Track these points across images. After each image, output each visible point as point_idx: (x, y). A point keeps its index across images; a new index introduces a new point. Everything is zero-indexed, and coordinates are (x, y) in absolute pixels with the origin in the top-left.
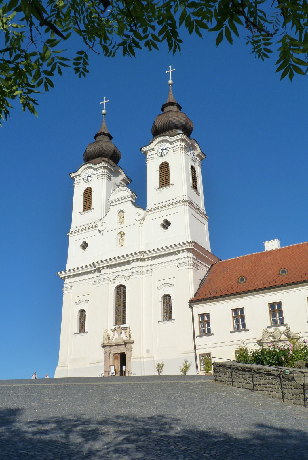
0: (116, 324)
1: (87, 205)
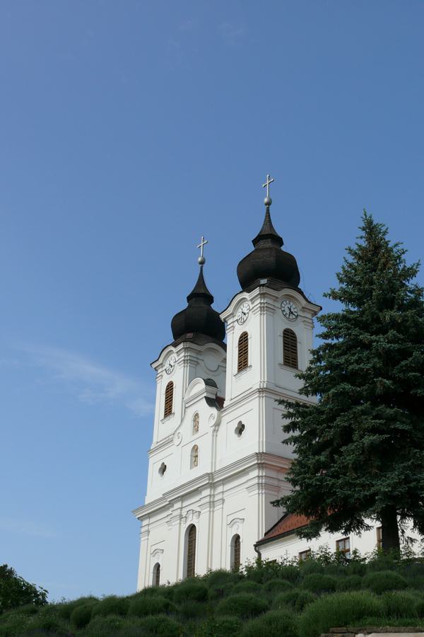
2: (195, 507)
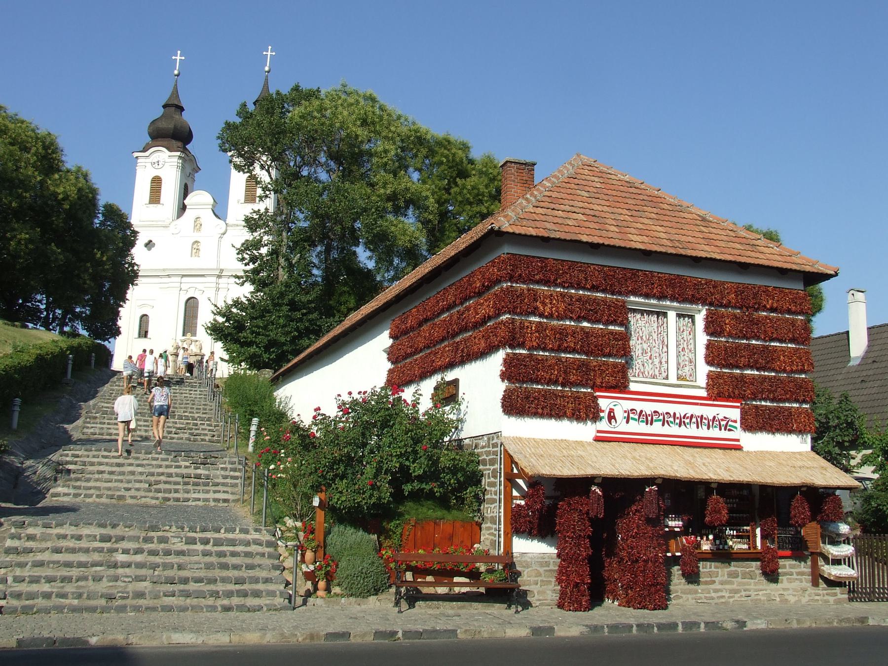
0: (184, 335)
1: (155, 196)
2: (200, 286)
